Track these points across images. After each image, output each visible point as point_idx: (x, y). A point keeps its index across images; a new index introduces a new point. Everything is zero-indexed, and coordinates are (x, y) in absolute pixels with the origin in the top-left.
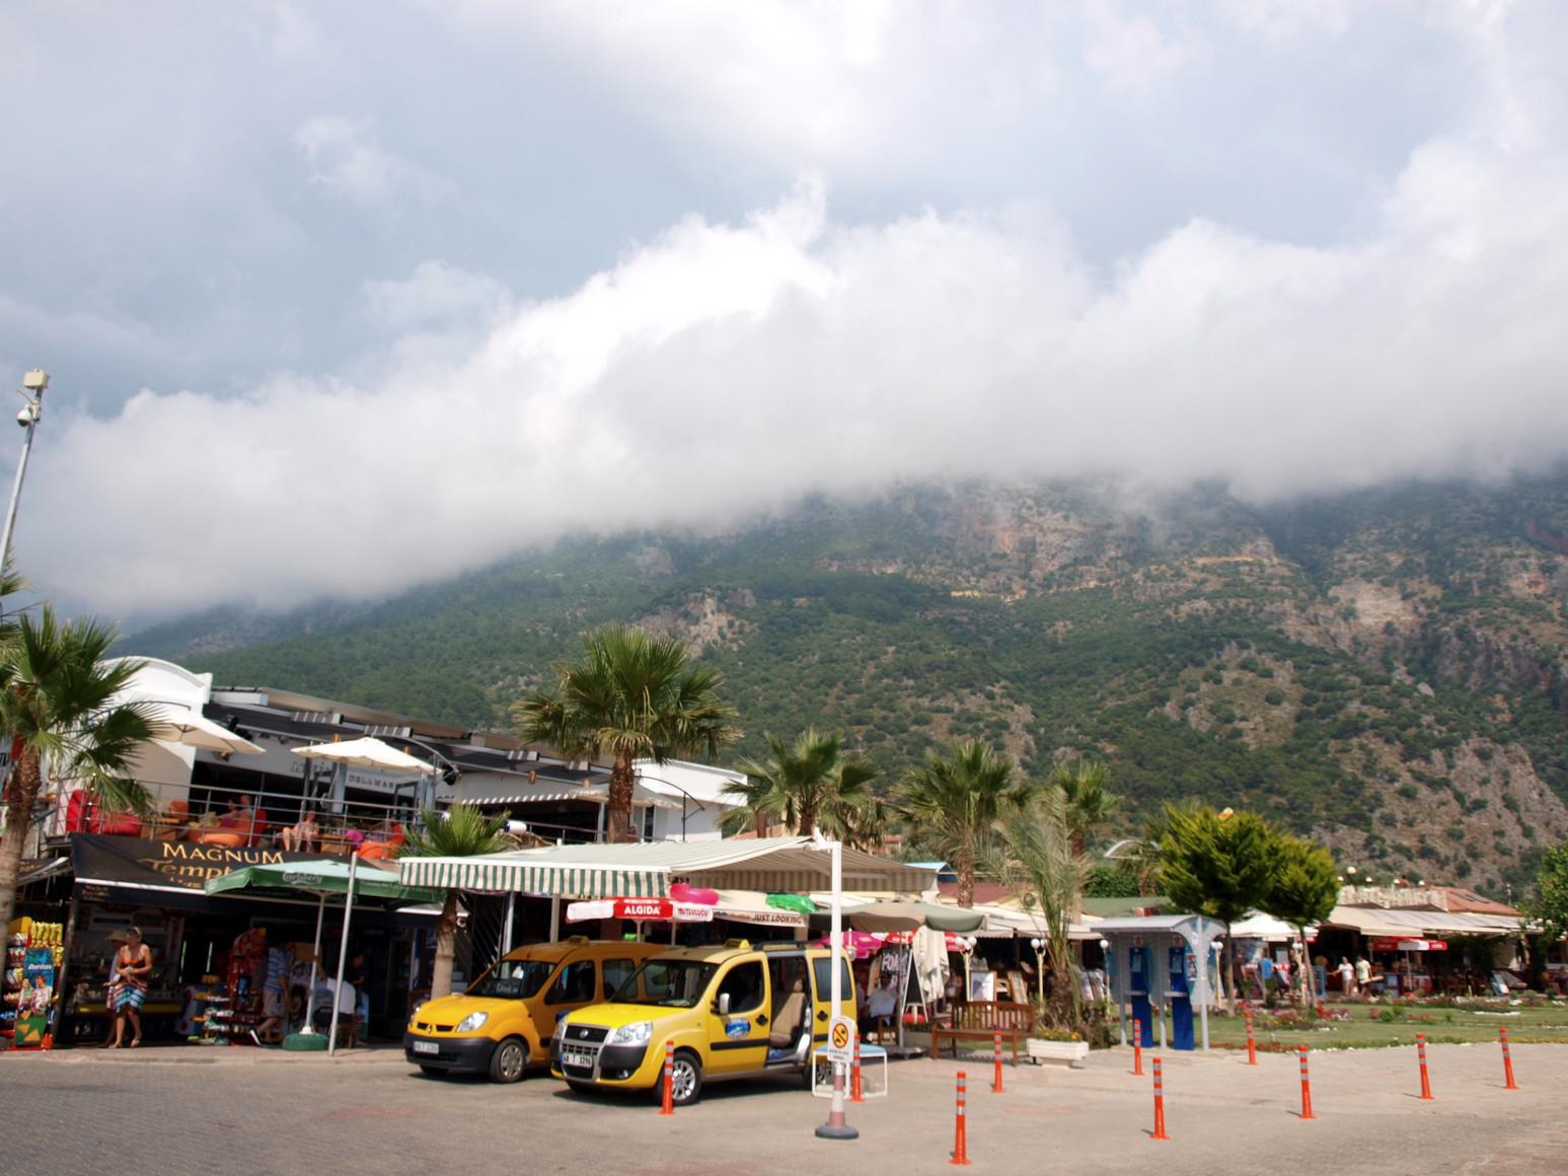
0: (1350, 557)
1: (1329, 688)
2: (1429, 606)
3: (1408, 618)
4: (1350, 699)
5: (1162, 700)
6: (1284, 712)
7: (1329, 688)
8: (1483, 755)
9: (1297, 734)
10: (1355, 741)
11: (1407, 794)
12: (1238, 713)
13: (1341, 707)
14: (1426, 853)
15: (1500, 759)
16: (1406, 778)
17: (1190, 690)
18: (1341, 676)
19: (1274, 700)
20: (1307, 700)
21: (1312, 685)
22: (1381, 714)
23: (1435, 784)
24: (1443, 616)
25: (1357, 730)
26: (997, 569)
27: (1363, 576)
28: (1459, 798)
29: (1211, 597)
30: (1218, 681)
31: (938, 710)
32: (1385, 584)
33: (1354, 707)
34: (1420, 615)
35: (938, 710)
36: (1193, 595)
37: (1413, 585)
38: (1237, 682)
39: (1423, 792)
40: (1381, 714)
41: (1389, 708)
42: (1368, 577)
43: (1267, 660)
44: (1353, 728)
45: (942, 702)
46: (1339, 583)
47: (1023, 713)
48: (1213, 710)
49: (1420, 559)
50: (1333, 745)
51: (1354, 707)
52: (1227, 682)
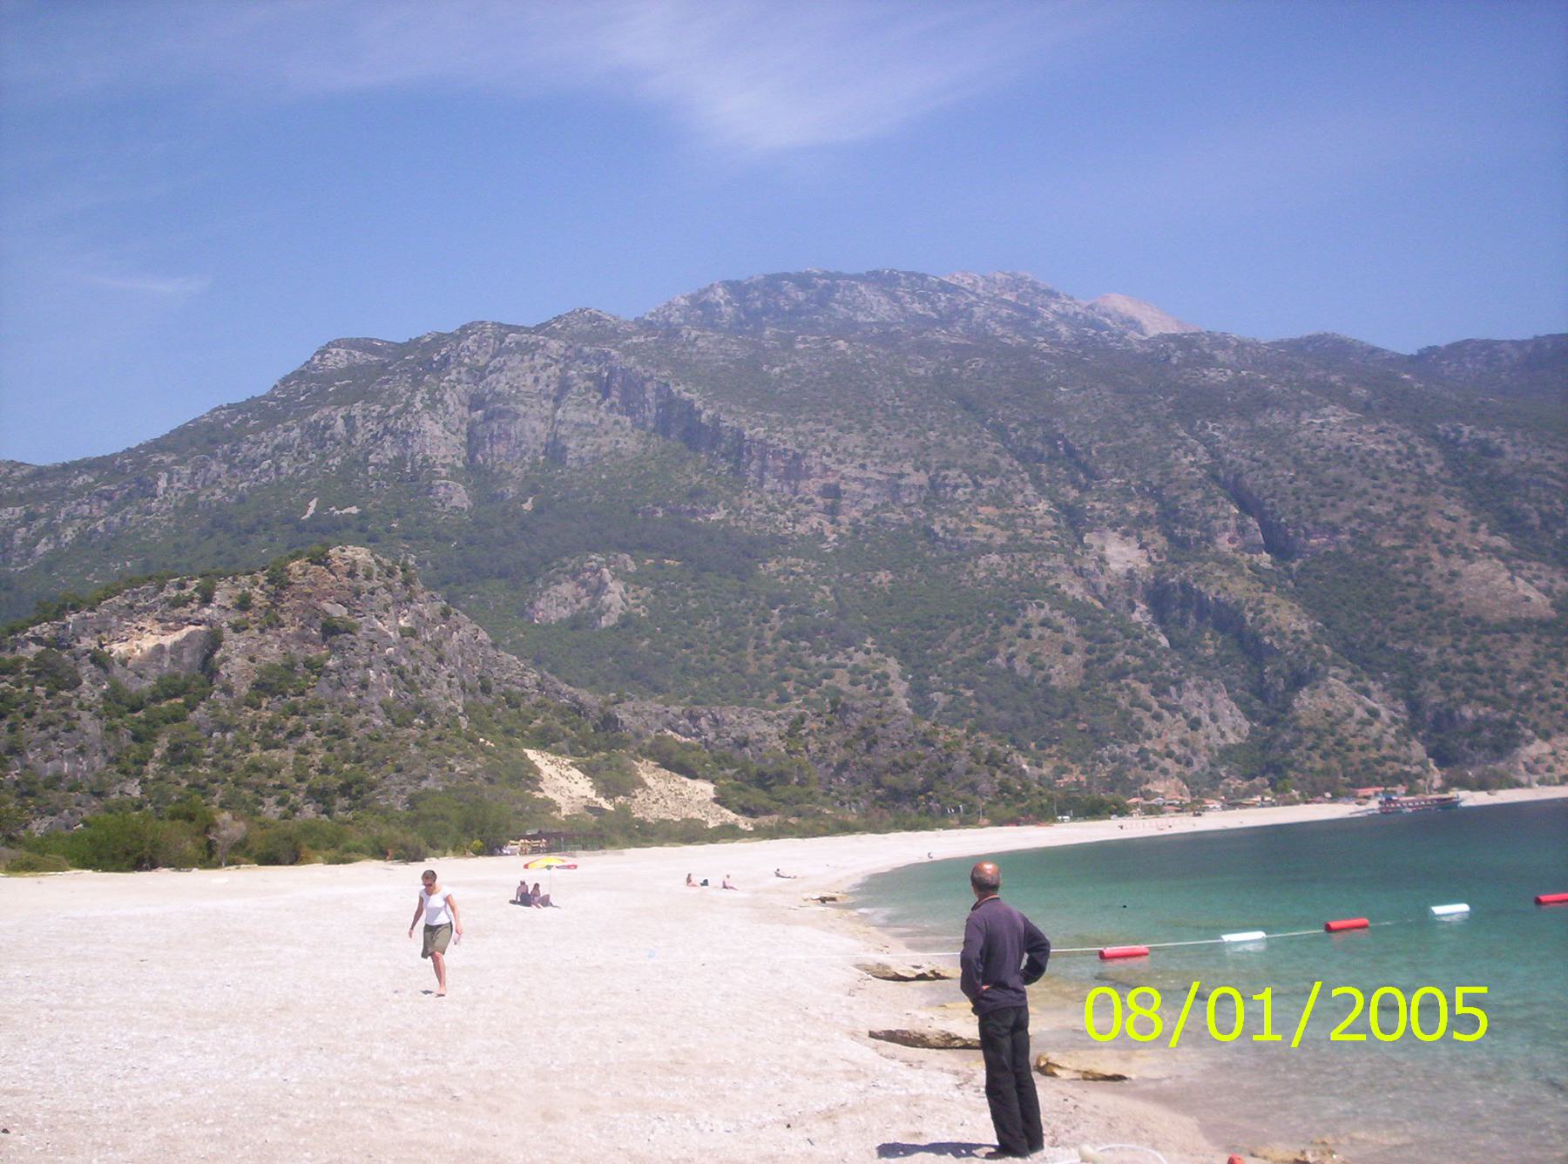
0: (1098, 505)
1: (1103, 641)
2: (1159, 557)
3: (1145, 565)
4: (1117, 650)
5: (994, 654)
6: (1076, 659)
7: (1103, 641)
8: (1199, 688)
9: (1087, 677)
10: (1123, 682)
11: (1157, 717)
12: (1047, 662)
13: (1112, 657)
14: (1170, 755)
15: (1208, 689)
16: (1155, 706)
17: (1010, 645)
18: (1110, 631)
19: (1067, 651)
20: (1089, 651)
21: (1088, 638)
22: (1138, 662)
23: (1173, 709)
24: (1169, 566)
25: (1125, 674)
26: (807, 515)
27: (1110, 525)
28: (1186, 716)
29: (1002, 550)
30: (1028, 637)
31: (838, 666)
32: (1126, 534)
33: (1120, 657)
34: (1154, 563)
35: (838, 666)
36: (986, 549)
37: (1147, 536)
38: (1041, 637)
39: (1166, 714)
40: (1138, 662)
41: (1144, 656)
42: (1114, 526)
43: (1058, 617)
44: (1120, 673)
45: (837, 660)
46: (1091, 531)
47: (893, 666)
48: (1029, 661)
49: (1151, 511)
50: (1111, 685)
51: (1120, 657)
52: (1035, 637)
